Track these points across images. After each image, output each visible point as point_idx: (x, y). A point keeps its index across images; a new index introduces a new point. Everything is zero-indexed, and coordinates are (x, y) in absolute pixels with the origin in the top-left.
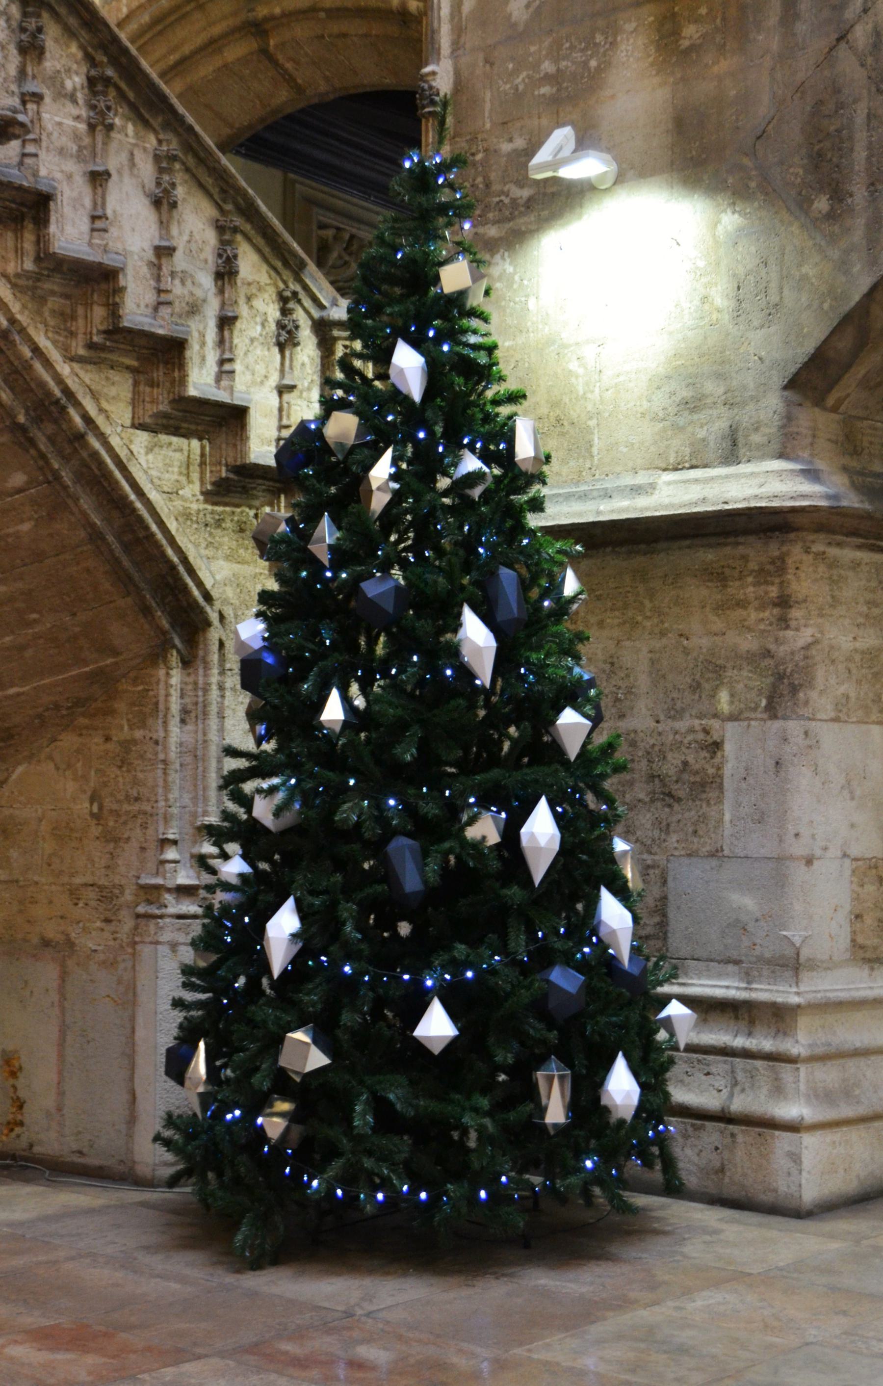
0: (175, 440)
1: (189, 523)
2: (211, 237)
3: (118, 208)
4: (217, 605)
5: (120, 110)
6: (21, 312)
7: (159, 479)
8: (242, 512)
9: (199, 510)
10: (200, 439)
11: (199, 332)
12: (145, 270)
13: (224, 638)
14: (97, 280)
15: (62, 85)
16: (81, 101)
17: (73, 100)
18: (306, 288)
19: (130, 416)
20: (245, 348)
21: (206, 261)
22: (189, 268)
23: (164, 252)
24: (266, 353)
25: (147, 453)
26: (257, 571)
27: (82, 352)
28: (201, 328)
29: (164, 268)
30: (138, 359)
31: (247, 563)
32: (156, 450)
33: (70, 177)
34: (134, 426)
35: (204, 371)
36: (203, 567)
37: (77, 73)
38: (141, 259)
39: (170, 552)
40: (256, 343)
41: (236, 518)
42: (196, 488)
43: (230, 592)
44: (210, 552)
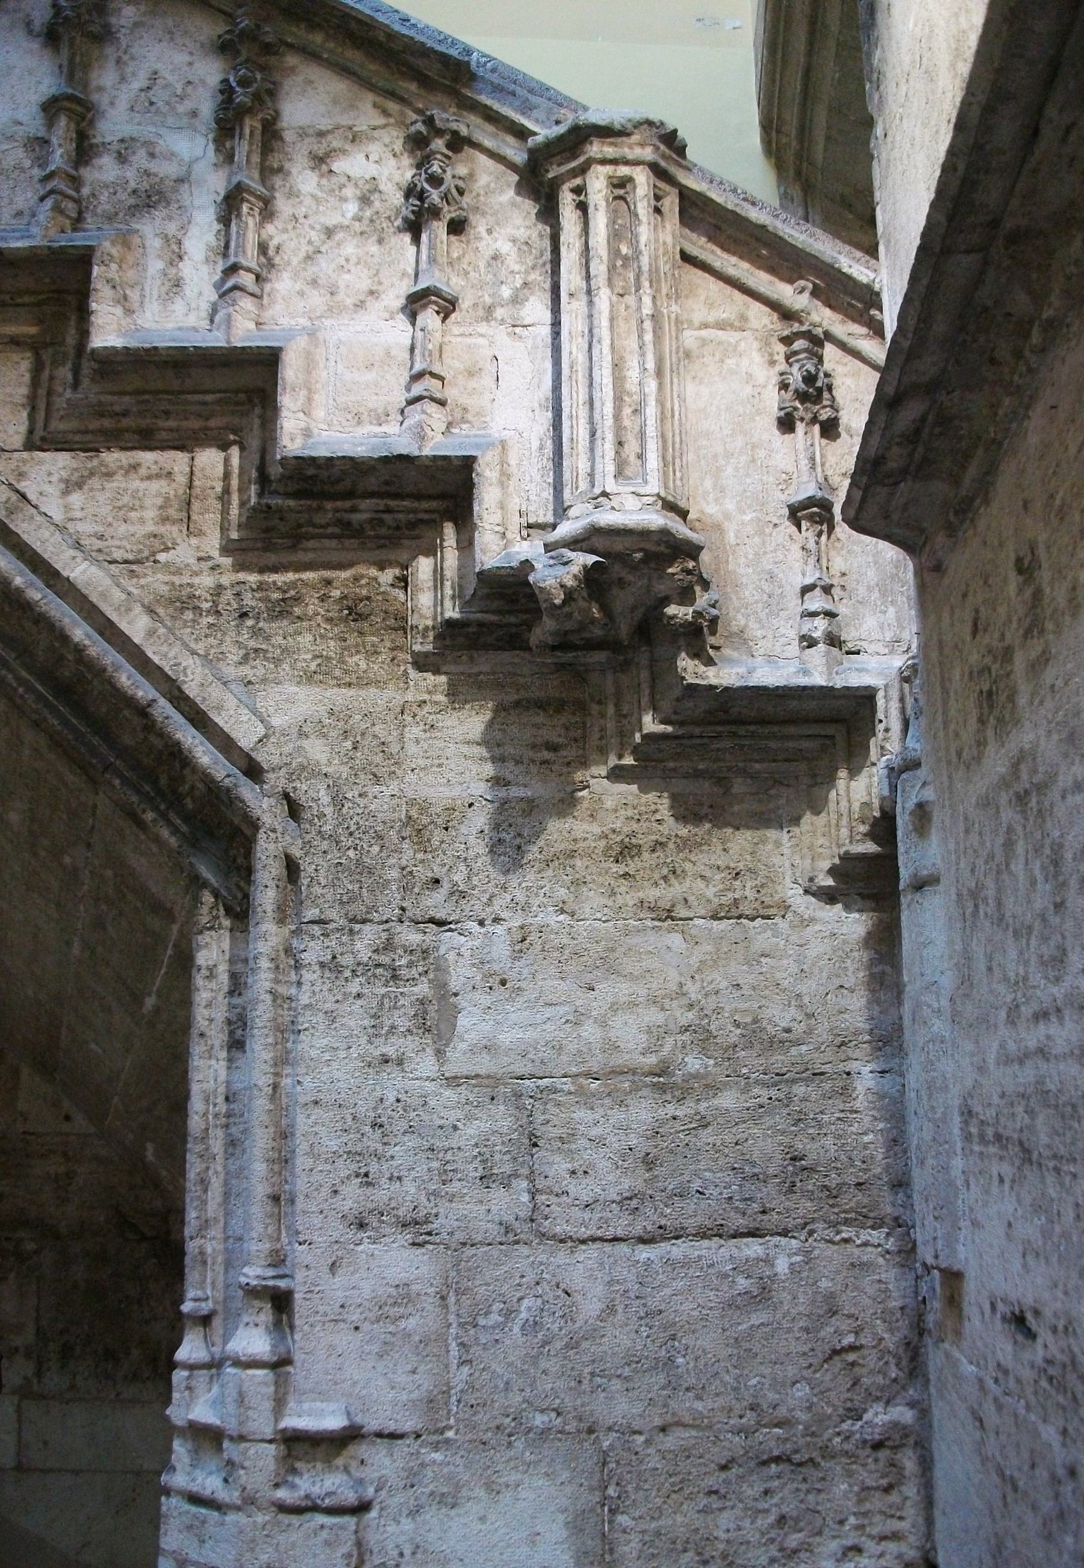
0: (148, 458)
1: (189, 615)
2: (211, 72)
4: (276, 780)
7: (101, 537)
8: (356, 579)
9: (219, 589)
10: (224, 447)
11: (166, 239)
13: (296, 852)
18: (492, 117)
19: (23, 428)
20: (305, 249)
21: (194, 114)
22: (146, 131)
24: (374, 249)
25: (66, 493)
26: (410, 696)
28: (172, 228)
29: (55, 141)
30: (40, 322)
31: (376, 683)
32: (95, 482)
34: (30, 445)
35: (179, 306)
36: (231, 702)
39: (128, 679)
40: (339, 236)
41: (336, 594)
42: (212, 543)
43: (317, 750)
44: (256, 670)
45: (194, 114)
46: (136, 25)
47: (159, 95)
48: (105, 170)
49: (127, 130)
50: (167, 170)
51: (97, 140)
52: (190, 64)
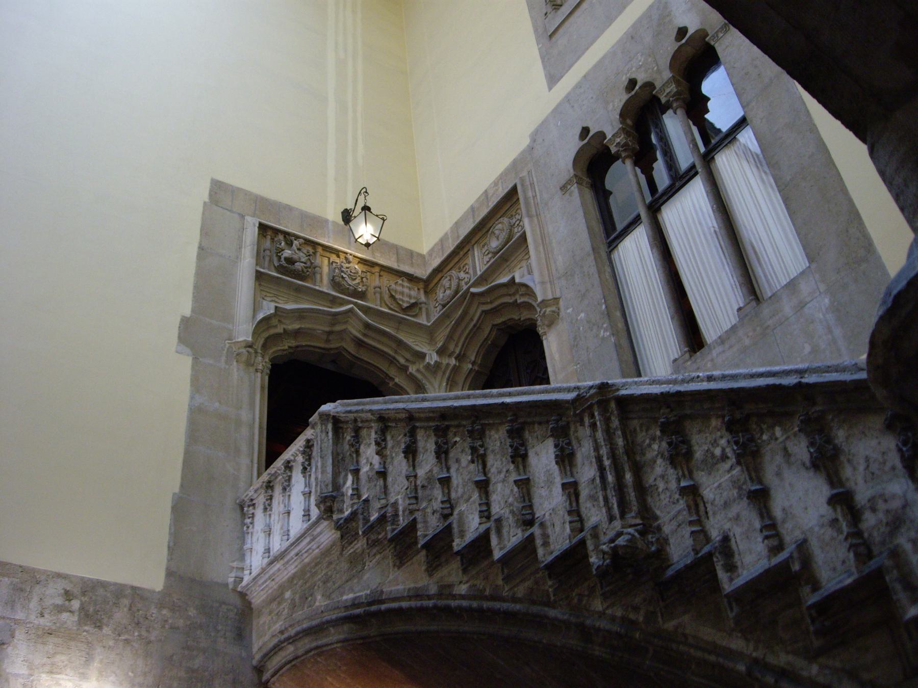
3: (787, 504)
5: (764, 427)
6: (756, 649)
12: (829, 532)
14: (786, 579)
15: (713, 455)
16: (729, 455)
17: (724, 457)
23: (842, 499)
27: (817, 643)
33: (737, 518)
37: (722, 437)
38: (822, 526)
45: (893, 468)
46: (847, 438)
47: (874, 467)
48: (869, 520)
49: (869, 494)
50: (896, 504)
51: (859, 506)
52: (879, 443)
